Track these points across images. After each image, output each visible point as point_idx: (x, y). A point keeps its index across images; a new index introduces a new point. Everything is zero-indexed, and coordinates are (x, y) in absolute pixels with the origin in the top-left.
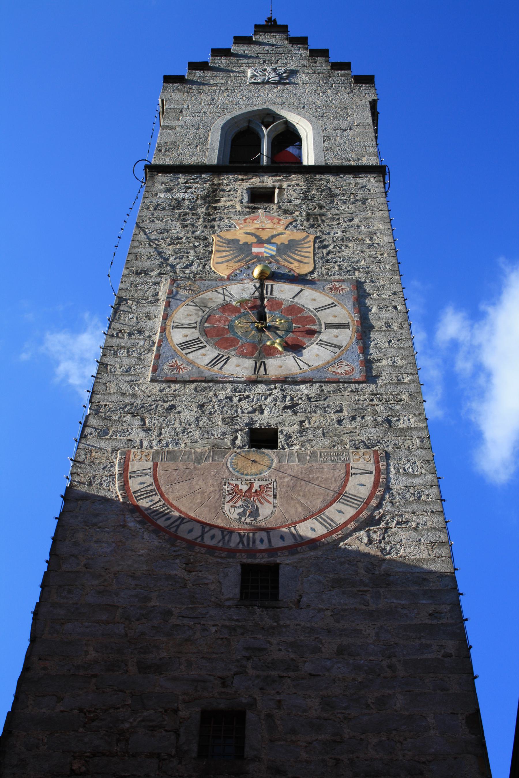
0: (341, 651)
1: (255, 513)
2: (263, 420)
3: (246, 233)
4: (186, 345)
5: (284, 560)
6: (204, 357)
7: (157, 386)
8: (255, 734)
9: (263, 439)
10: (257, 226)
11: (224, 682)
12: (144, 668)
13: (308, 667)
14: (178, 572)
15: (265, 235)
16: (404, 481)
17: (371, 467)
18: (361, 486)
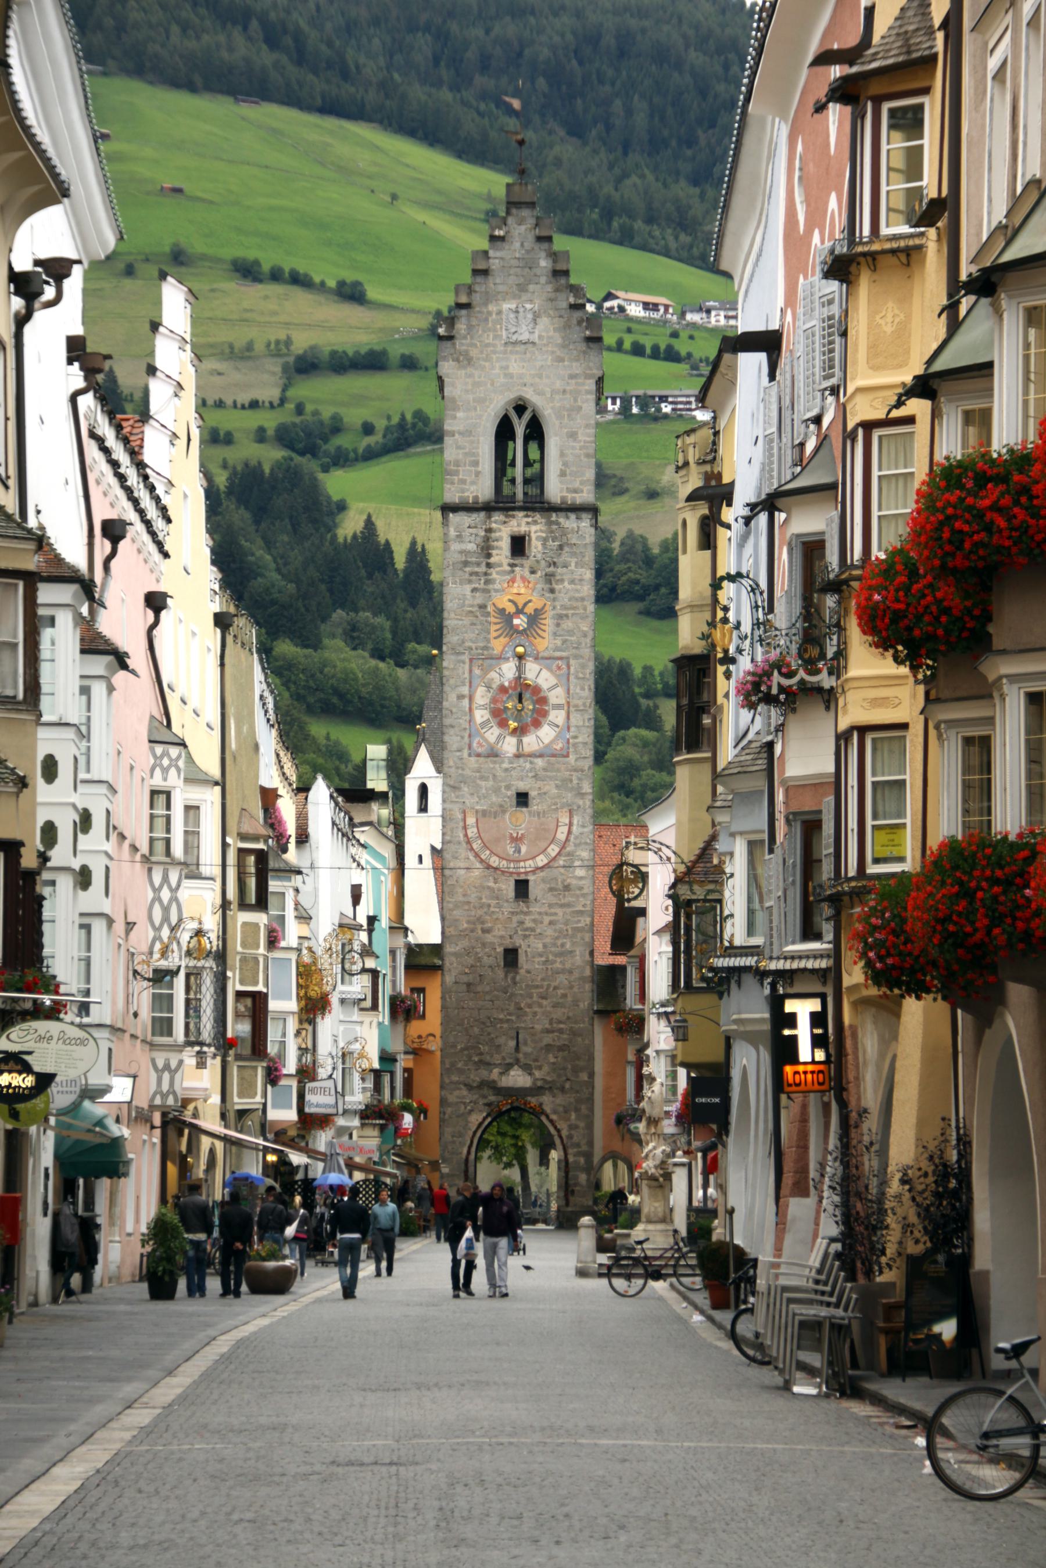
0: (551, 923)
1: (519, 852)
2: (522, 786)
3: (510, 601)
4: (484, 724)
5: (531, 878)
6: (493, 734)
7: (473, 759)
8: (522, 958)
9: (522, 799)
10: (515, 591)
11: (511, 937)
12: (484, 931)
13: (538, 931)
14: (491, 884)
15: (520, 603)
16: (581, 830)
17: (567, 821)
18: (561, 835)
